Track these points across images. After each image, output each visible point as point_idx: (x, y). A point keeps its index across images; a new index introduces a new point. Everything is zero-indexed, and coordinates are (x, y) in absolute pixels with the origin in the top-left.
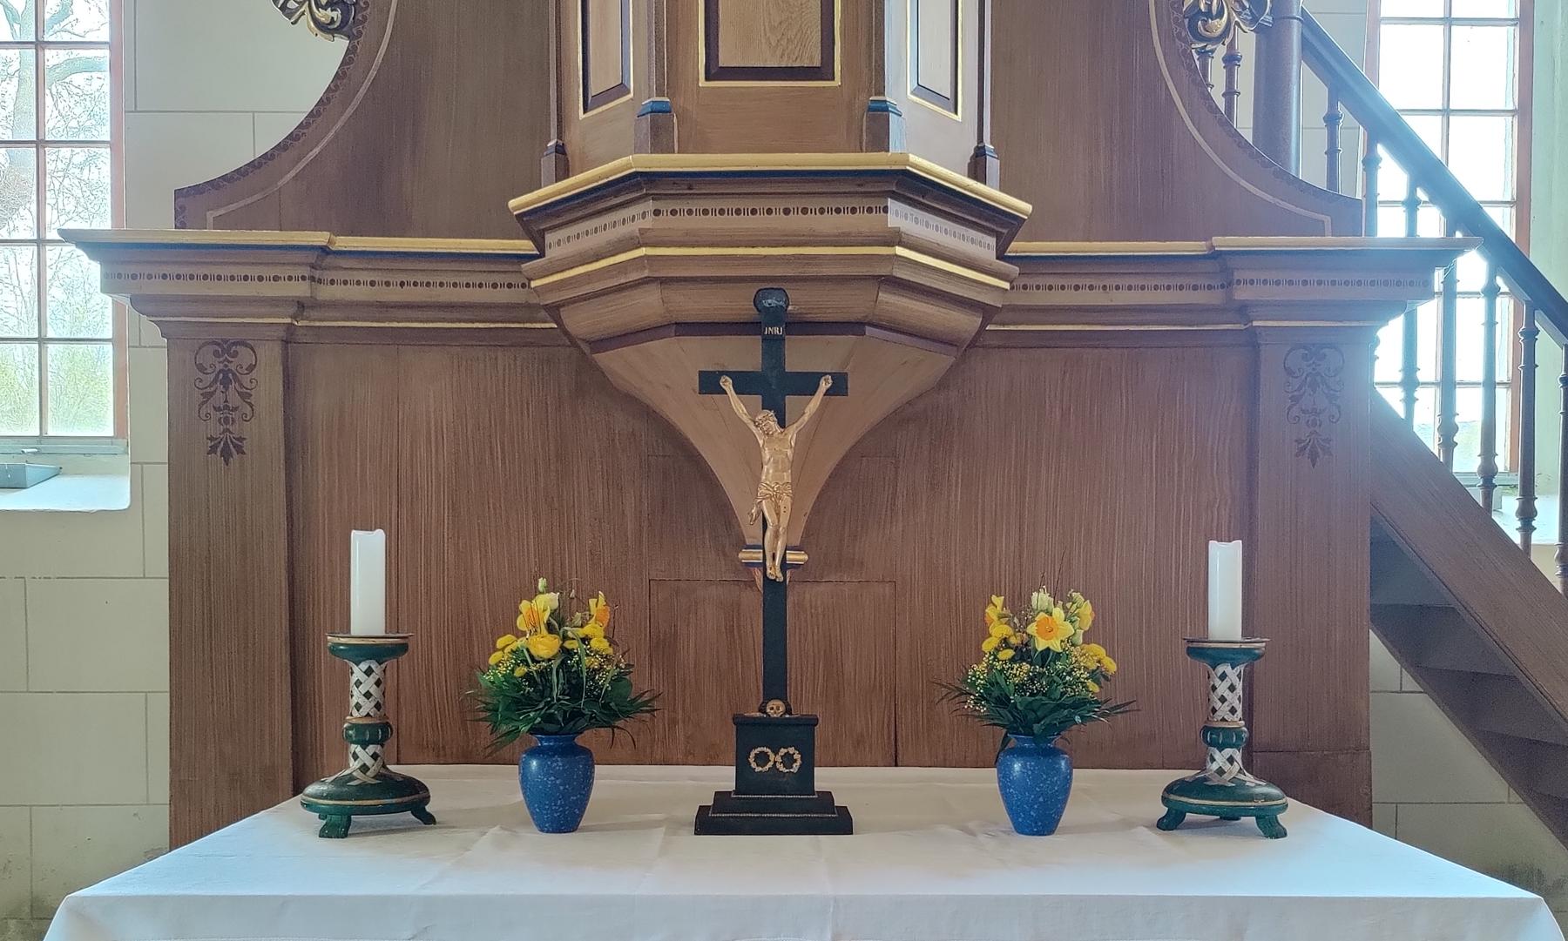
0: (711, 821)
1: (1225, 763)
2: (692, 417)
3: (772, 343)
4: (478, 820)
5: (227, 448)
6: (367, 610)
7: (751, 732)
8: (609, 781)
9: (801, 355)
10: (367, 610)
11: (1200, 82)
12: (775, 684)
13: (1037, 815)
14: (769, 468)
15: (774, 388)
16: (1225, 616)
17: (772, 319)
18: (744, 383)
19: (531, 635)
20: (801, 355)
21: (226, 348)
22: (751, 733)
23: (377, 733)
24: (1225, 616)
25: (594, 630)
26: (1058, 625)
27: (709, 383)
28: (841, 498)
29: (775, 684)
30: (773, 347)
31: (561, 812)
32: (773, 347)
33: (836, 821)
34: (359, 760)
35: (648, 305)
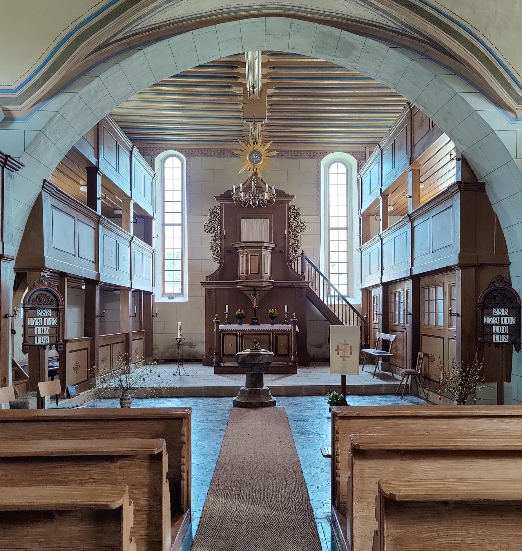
1: (286, 321)
2: (249, 296)
3: (255, 291)
6: (227, 311)
7: (253, 319)
10: (227, 311)
11: (291, 266)
12: (255, 316)
14: (255, 300)
15: (255, 295)
16: (286, 311)
17: (255, 290)
18: (253, 295)
21: (210, 290)
23: (227, 319)
24: (286, 311)
26: (273, 311)
27: (250, 295)
28: (260, 302)
29: (255, 316)
30: (255, 292)
32: (255, 292)
34: (226, 321)
35: (246, 289)
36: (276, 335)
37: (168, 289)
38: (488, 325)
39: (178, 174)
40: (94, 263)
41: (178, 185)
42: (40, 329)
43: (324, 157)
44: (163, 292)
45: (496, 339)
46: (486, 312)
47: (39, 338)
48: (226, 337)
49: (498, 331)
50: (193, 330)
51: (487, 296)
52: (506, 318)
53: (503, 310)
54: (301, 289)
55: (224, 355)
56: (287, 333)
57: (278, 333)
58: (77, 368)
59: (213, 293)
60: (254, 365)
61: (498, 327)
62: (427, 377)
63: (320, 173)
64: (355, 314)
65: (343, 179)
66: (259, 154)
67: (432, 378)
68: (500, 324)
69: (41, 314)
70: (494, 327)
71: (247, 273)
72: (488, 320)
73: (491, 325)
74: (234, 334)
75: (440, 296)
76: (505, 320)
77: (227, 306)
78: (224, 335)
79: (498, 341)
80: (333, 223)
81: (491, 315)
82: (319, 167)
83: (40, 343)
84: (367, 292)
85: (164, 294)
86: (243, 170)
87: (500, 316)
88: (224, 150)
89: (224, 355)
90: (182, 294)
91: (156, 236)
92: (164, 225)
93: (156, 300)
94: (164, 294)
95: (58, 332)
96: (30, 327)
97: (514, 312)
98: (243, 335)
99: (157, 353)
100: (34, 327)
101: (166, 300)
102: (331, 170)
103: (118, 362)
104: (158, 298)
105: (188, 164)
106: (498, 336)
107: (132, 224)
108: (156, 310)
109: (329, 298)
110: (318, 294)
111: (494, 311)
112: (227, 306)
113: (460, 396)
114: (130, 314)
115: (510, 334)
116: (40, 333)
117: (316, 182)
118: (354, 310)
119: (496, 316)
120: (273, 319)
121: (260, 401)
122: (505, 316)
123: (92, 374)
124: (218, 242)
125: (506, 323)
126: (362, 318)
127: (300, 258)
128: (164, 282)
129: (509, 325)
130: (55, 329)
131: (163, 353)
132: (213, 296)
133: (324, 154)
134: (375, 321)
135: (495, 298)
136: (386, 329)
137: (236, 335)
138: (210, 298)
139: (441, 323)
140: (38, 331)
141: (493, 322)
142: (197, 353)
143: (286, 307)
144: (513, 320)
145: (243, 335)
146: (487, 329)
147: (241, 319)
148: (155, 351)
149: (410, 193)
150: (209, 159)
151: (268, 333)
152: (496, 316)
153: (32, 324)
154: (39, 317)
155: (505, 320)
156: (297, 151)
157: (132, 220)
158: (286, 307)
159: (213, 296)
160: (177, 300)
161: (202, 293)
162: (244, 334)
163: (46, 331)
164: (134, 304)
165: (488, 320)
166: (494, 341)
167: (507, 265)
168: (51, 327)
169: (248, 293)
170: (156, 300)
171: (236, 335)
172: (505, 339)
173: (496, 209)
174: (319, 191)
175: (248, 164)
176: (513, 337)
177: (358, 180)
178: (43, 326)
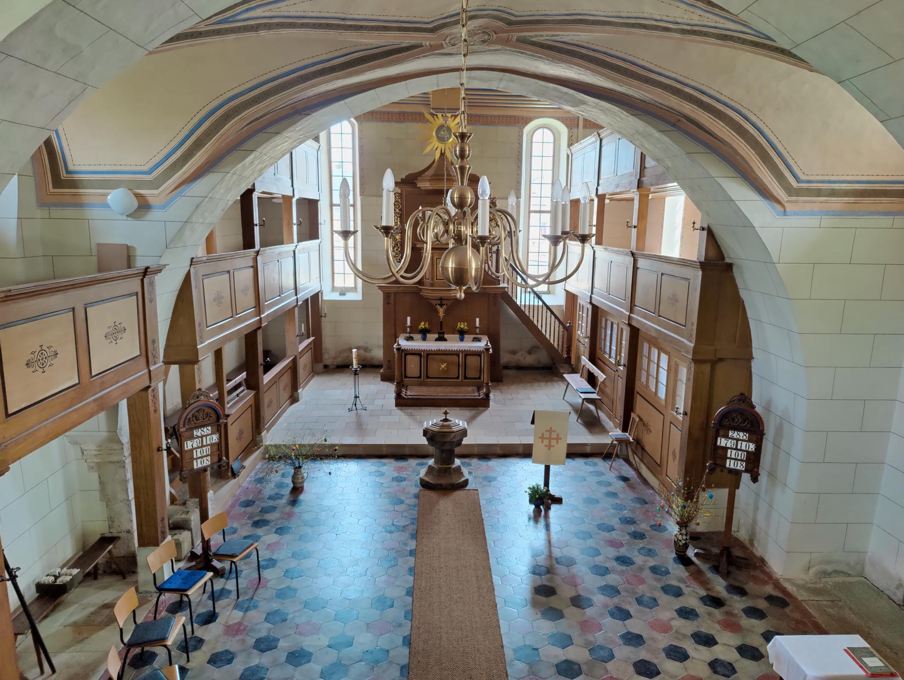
0: (437, 340)
4: (418, 340)
5: (388, 303)
6: (409, 323)
8: (428, 335)
9: (444, 302)
10: (409, 323)
13: (462, 340)
14: (441, 311)
15: (441, 305)
16: (477, 324)
17: (441, 299)
19: (422, 325)
20: (444, 302)
21: (389, 294)
22: (439, 333)
24: (477, 324)
25: (427, 326)
31: (424, 339)
33: (445, 340)
36: (466, 356)
37: (339, 283)
38: (723, 447)
39: (348, 141)
40: (252, 267)
41: (348, 155)
42: (199, 450)
43: (527, 123)
44: (333, 286)
45: (730, 464)
46: (721, 432)
47: (199, 461)
48: (409, 357)
49: (733, 456)
50: (368, 334)
51: (724, 415)
52: (744, 443)
53: (741, 434)
54: (495, 294)
55: (406, 377)
56: (478, 354)
57: (468, 354)
58: (240, 438)
59: (392, 297)
60: (445, 442)
61: (734, 452)
62: (638, 443)
63: (521, 145)
64: (557, 322)
65: (549, 150)
66: (449, 129)
67: (646, 448)
68: (736, 449)
69: (199, 434)
70: (729, 451)
71: (433, 279)
72: (722, 442)
73: (725, 449)
74: (417, 353)
75: (664, 363)
76: (743, 446)
77: (409, 318)
78: (406, 355)
79: (732, 466)
80: (535, 205)
81: (726, 436)
82: (521, 136)
83: (200, 466)
84: (571, 298)
85: (334, 289)
86: (428, 149)
87: (737, 440)
88: (404, 113)
89: (406, 377)
90: (355, 289)
91: (323, 222)
92: (332, 205)
93: (325, 298)
94: (334, 289)
95: (219, 449)
96: (186, 451)
97: (755, 438)
98: (428, 355)
99: (328, 358)
100: (191, 451)
101: (336, 296)
102: (534, 140)
103: (285, 395)
104: (328, 296)
105: (360, 131)
106: (732, 461)
107: (295, 227)
108: (325, 309)
109: (527, 295)
110: (514, 299)
111: (730, 433)
112: (409, 318)
113: (682, 516)
114: (297, 333)
115: (748, 461)
116: (199, 455)
117: (515, 158)
118: (559, 320)
119: (733, 439)
120: (462, 334)
121: (451, 482)
122: (744, 441)
123: (258, 425)
124: (398, 237)
125: (743, 448)
126: (564, 327)
127: (494, 256)
128: (333, 273)
129: (748, 452)
130: (216, 448)
131: (335, 358)
132: (392, 301)
133: (527, 121)
134: (579, 332)
135: (733, 420)
136: (593, 359)
137: (420, 355)
138: (388, 303)
139: (662, 394)
140: (197, 453)
141: (729, 445)
142: (373, 358)
143: (478, 320)
144: (752, 447)
145: (428, 355)
146: (720, 452)
147: (424, 333)
148: (326, 356)
149: (635, 223)
150: (386, 124)
151: (456, 353)
152: (733, 439)
153: (190, 447)
154: (198, 437)
155: (743, 446)
156: (495, 116)
157: (295, 221)
158: (478, 320)
159: (392, 301)
160: (350, 297)
161: (380, 295)
162: (429, 354)
163: (207, 450)
164: (300, 322)
165: (722, 442)
166: (727, 466)
167: (750, 358)
168: (212, 445)
169: (434, 302)
170: (325, 298)
171: (420, 355)
172: (741, 466)
173: (743, 294)
174: (519, 167)
175: (435, 143)
176: (750, 465)
177: (568, 156)
178: (203, 446)
